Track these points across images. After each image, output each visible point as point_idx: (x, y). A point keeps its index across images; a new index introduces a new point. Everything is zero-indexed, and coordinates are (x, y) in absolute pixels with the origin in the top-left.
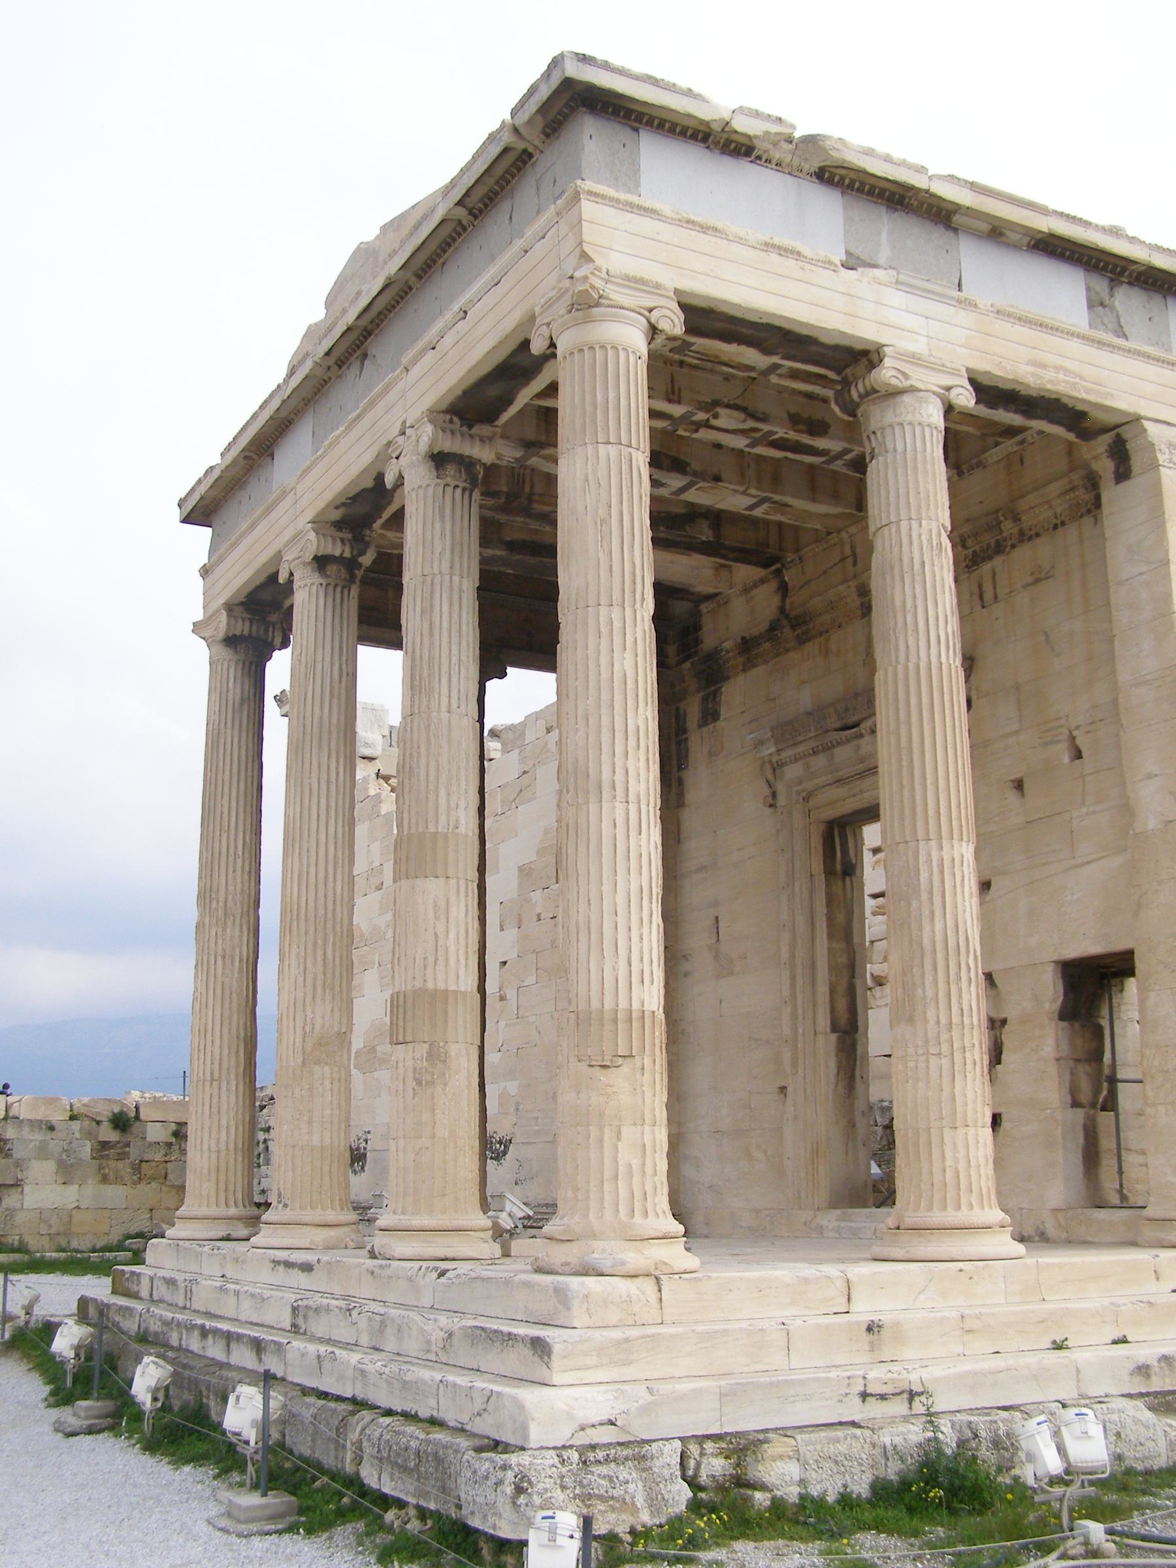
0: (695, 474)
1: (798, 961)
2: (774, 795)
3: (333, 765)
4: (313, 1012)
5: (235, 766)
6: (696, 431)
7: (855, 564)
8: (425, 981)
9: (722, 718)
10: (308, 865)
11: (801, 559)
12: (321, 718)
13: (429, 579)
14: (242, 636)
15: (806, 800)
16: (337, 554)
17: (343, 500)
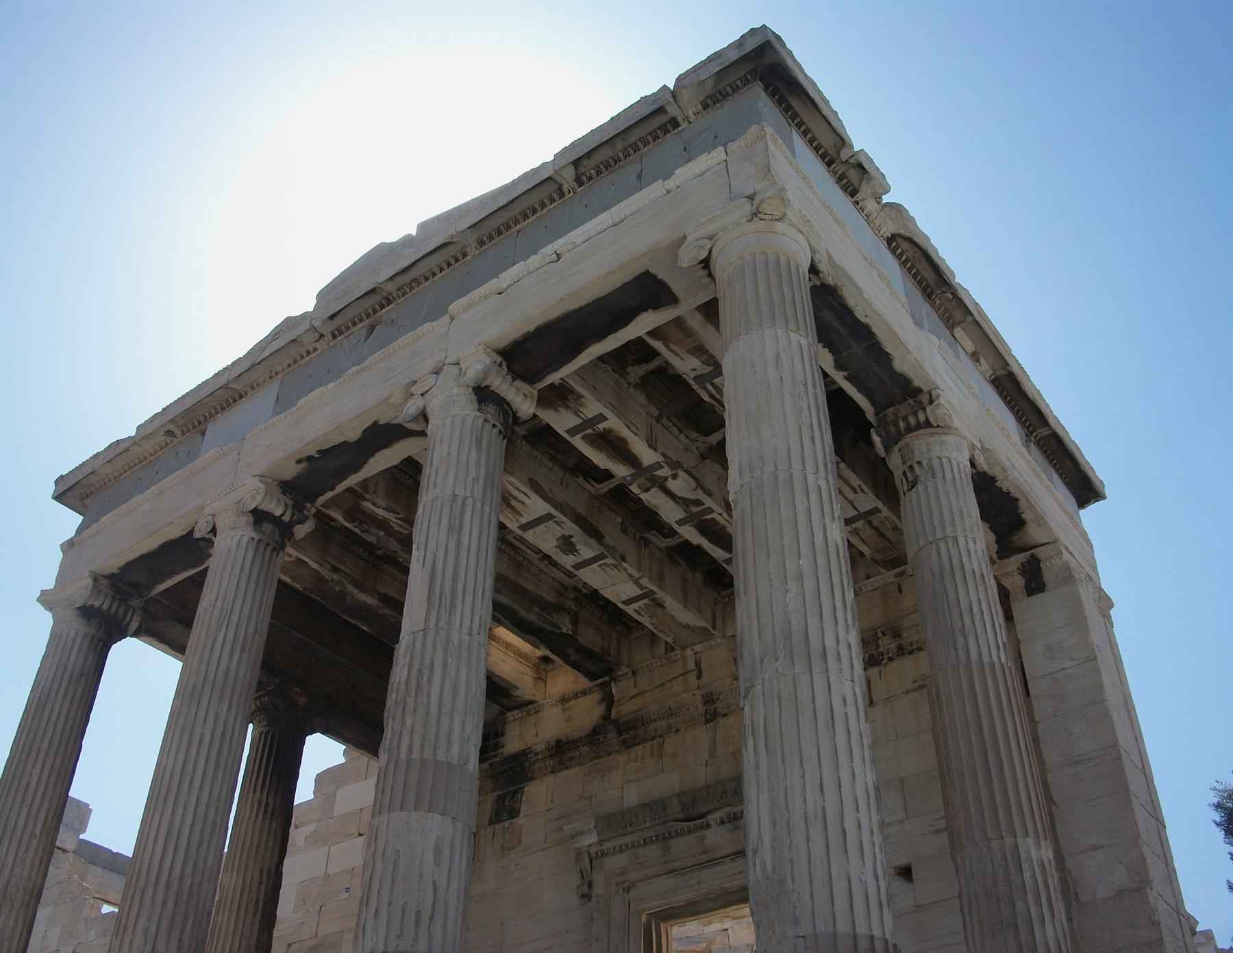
0: (607, 547)
2: (590, 885)
3: (231, 720)
5: (56, 739)
6: (647, 490)
7: (699, 677)
8: (416, 940)
9: (522, 814)
10: (182, 823)
11: (634, 673)
12: (228, 668)
13: (460, 500)
14: (99, 610)
15: (627, 890)
16: (278, 513)
17: (313, 453)
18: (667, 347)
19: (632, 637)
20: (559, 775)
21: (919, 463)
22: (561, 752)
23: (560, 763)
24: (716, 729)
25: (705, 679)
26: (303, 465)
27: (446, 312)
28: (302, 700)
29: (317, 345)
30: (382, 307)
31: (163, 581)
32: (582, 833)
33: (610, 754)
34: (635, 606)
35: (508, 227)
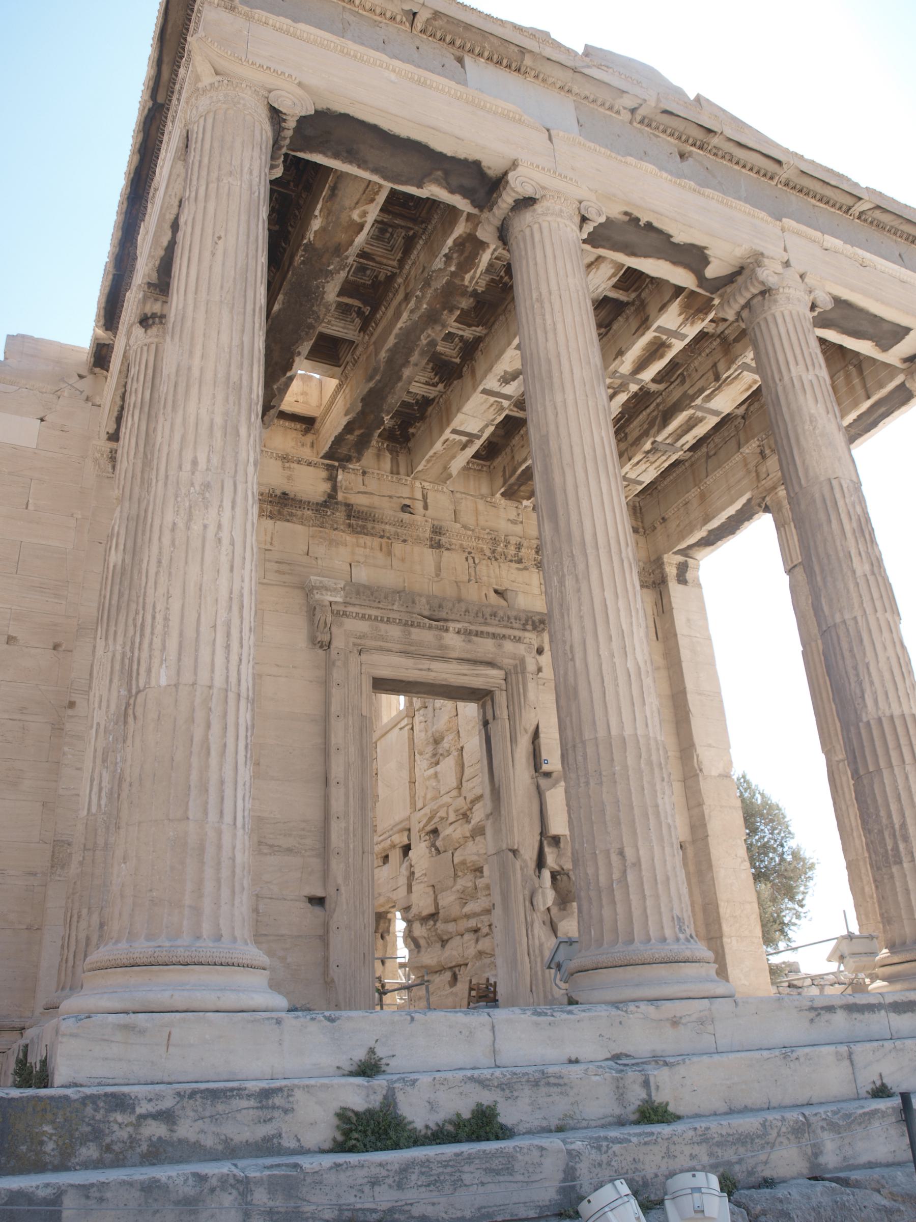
7: (426, 507)
11: (364, 473)
20: (278, 522)
23: (280, 513)
29: (623, 112)
31: (336, 156)
32: (327, 589)
33: (335, 529)
35: (807, 194)
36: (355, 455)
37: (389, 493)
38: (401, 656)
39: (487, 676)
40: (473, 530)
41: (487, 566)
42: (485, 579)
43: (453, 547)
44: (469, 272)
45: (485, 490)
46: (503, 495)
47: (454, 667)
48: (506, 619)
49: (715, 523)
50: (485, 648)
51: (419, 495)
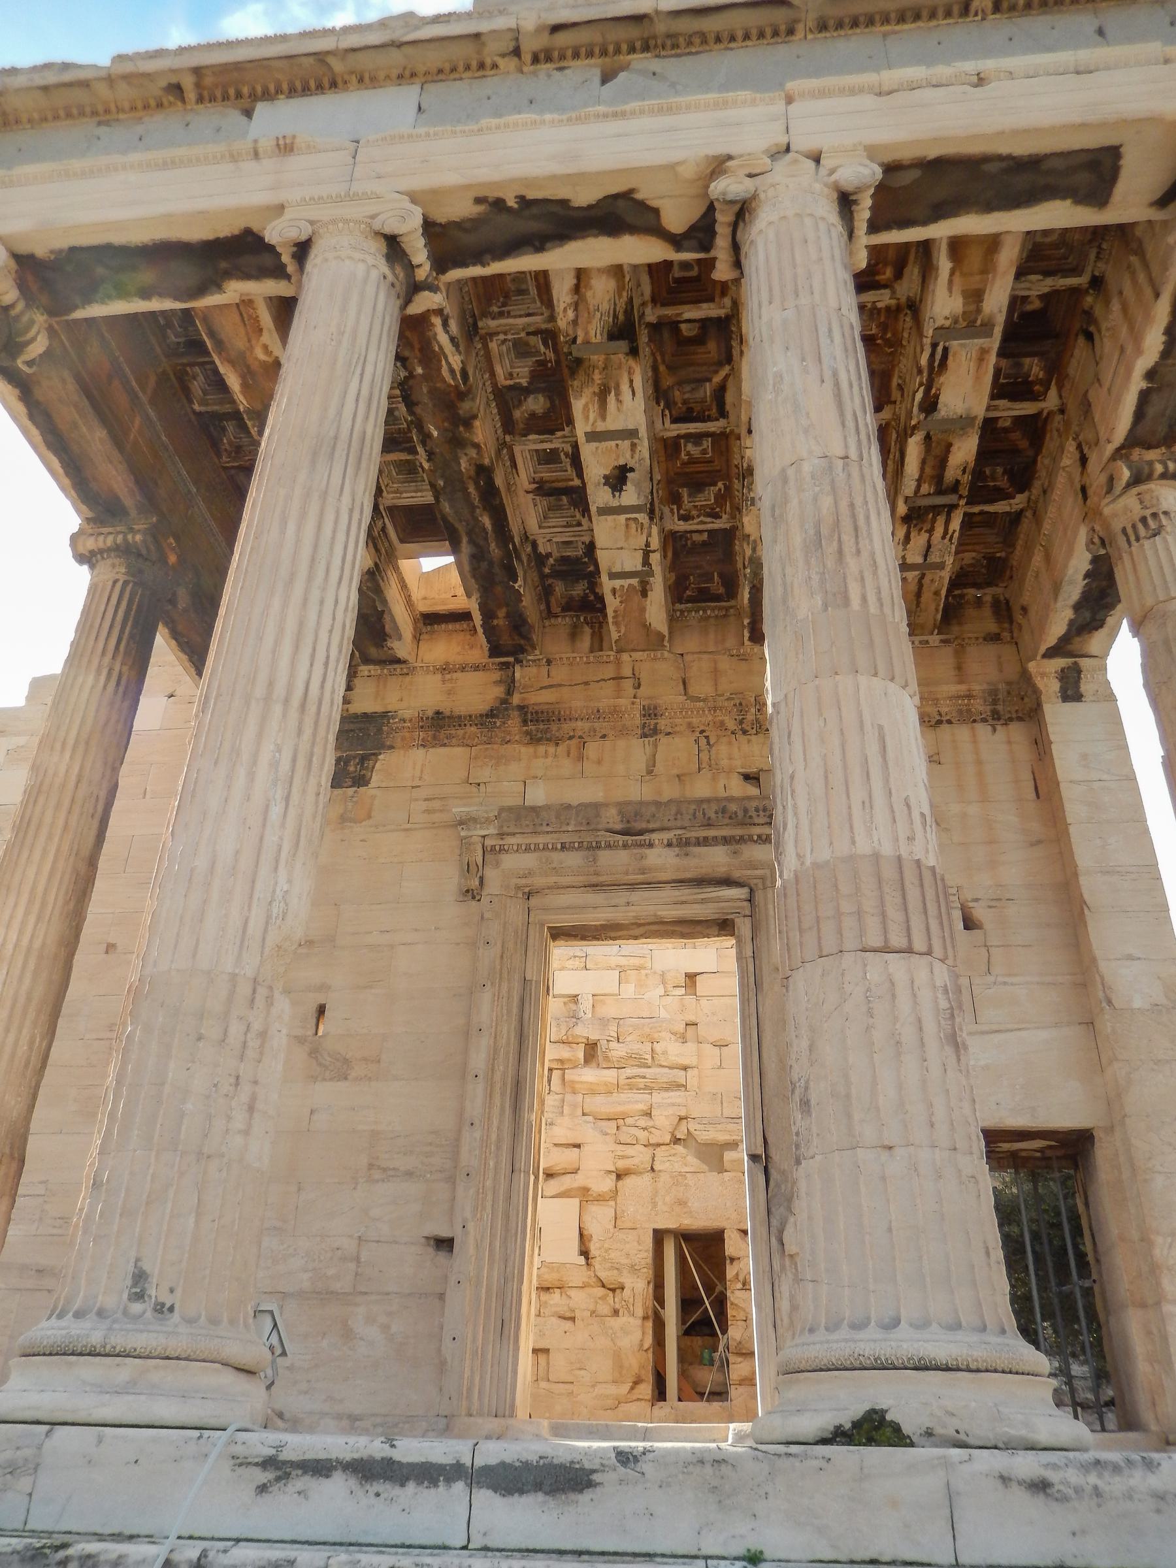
1: (498, 1076)
4: (290, 881)
9: (373, 784)
11: (549, 662)
15: (528, 896)
18: (952, 273)
19: (547, 623)
21: (1166, 513)
22: (439, 726)
23: (434, 737)
24: (656, 746)
25: (642, 691)
26: (480, 208)
27: (781, 85)
28: (172, 559)
29: (501, 62)
30: (632, 50)
34: (617, 583)
36: (522, 642)
37: (585, 679)
38: (588, 892)
39: (718, 900)
40: (704, 700)
41: (730, 743)
42: (724, 762)
43: (677, 729)
44: (441, 366)
45: (731, 642)
46: (750, 639)
47: (668, 893)
48: (740, 814)
49: (1074, 589)
50: (716, 859)
51: (627, 671)
